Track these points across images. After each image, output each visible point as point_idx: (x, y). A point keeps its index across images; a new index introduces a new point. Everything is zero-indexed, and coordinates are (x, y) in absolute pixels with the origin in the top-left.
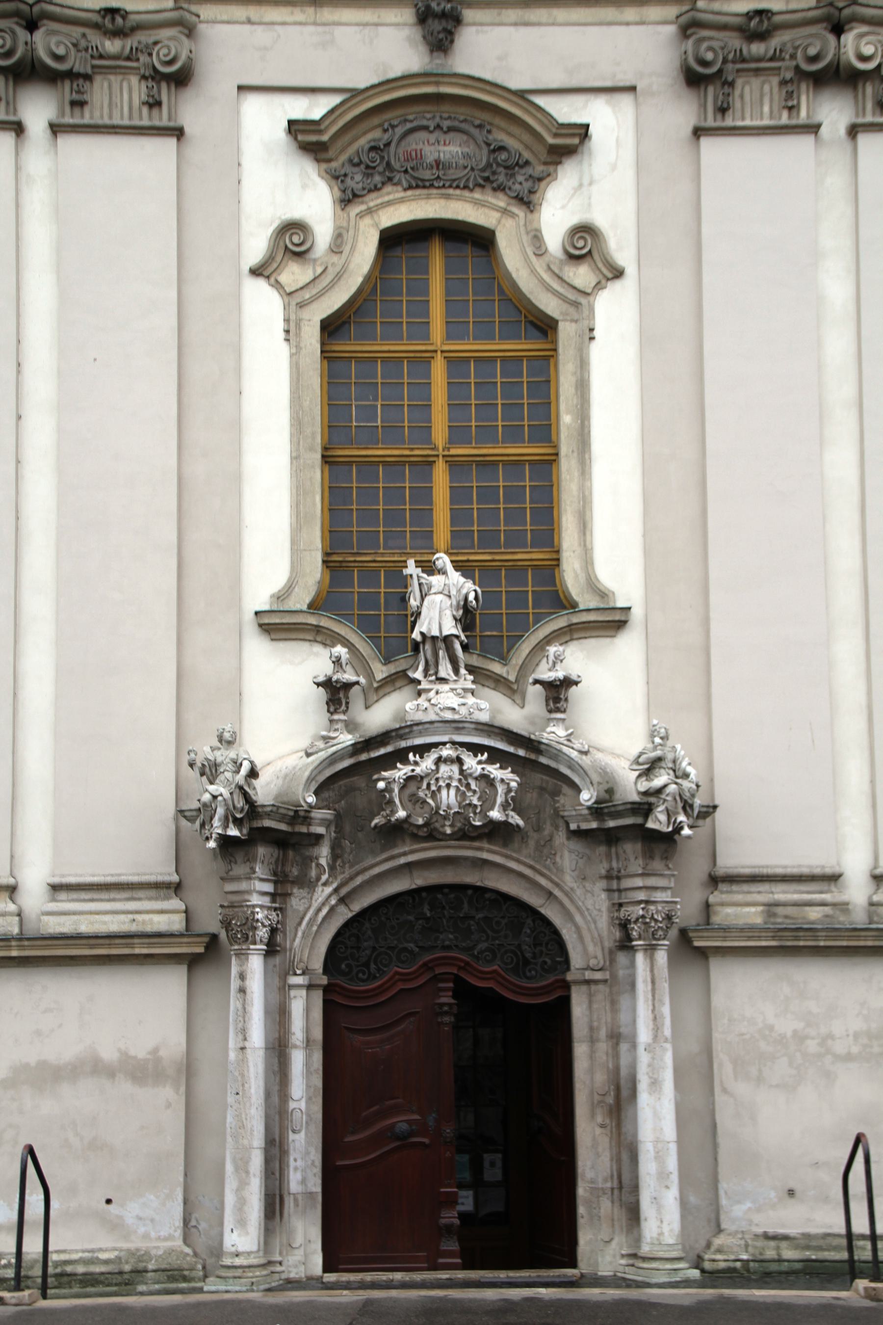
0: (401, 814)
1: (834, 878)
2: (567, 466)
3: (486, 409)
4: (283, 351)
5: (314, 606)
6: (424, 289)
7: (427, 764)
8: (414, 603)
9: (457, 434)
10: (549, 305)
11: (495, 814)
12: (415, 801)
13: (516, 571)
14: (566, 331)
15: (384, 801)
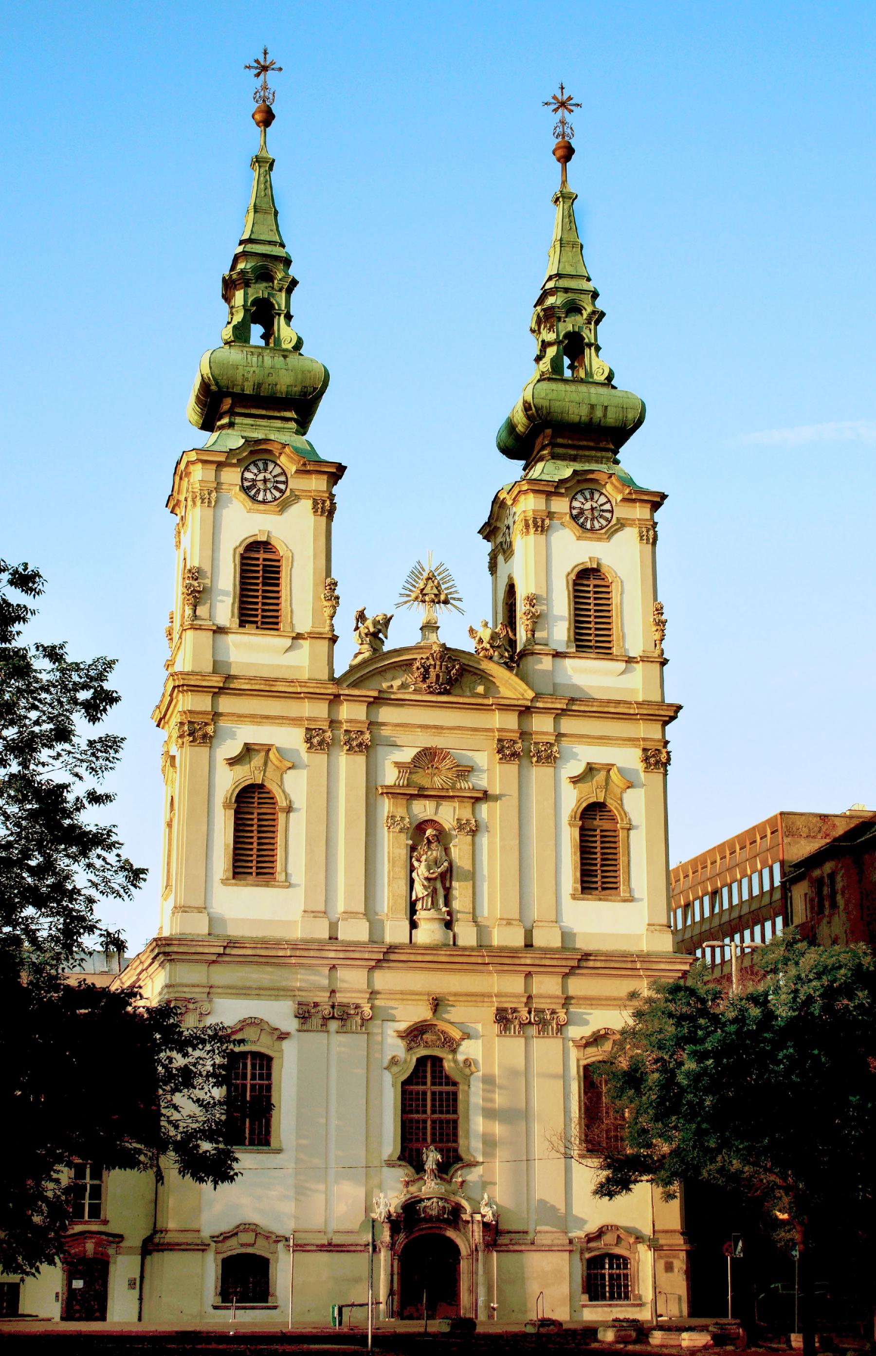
0: (423, 1215)
1: (526, 1232)
2: (461, 1122)
3: (441, 1106)
4: (392, 1089)
5: (399, 1159)
6: (425, 1071)
7: (428, 1203)
8: (425, 1159)
9: (433, 1112)
10: (458, 1079)
11: (446, 1216)
12: (424, 1212)
13: (448, 1150)
14: (462, 1087)
15: (418, 1212)
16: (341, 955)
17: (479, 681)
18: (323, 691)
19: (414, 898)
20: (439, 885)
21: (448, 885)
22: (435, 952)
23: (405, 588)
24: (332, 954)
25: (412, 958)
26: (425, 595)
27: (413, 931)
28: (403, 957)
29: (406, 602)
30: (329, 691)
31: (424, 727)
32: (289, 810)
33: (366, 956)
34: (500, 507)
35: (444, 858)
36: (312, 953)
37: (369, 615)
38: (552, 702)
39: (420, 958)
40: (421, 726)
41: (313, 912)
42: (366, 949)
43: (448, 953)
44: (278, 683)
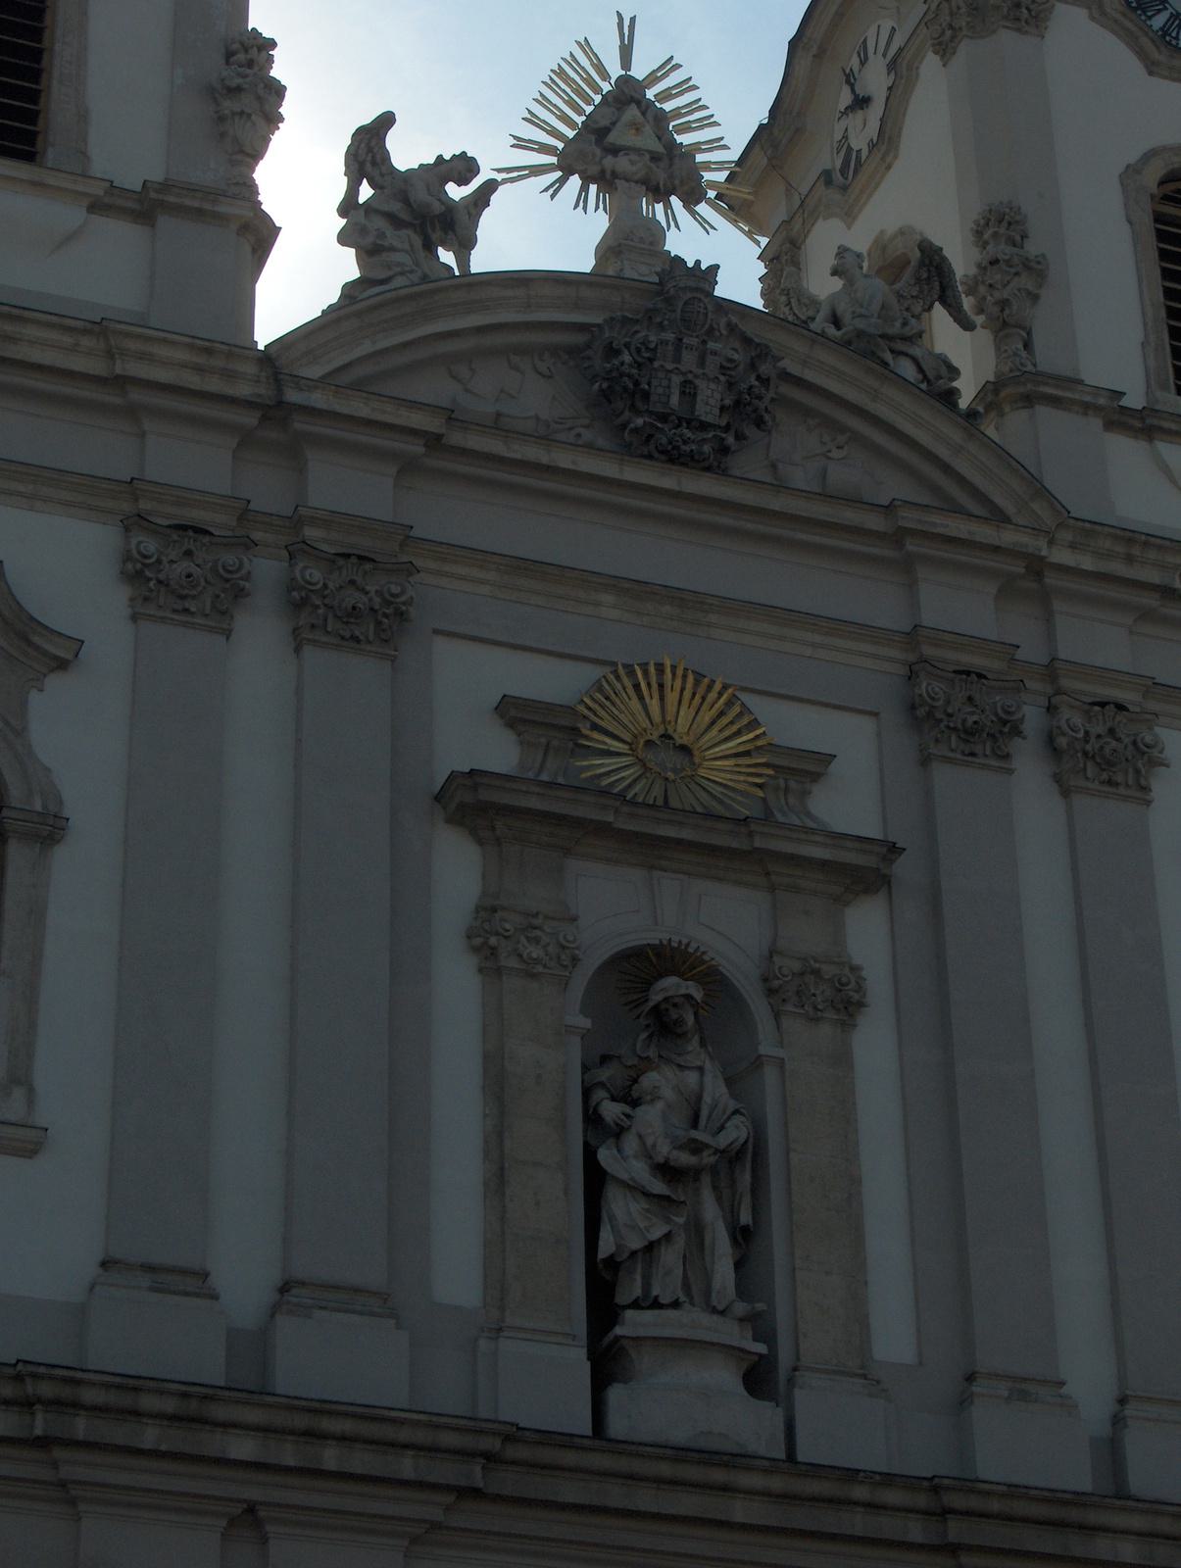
16: (288, 1454)
17: (836, 454)
18: (214, 385)
19: (606, 1246)
20: (711, 1211)
21: (745, 1218)
22: (718, 1476)
23: (532, 120)
24: (243, 1448)
25: (616, 1495)
26: (615, 151)
27: (615, 1394)
28: (570, 1491)
29: (536, 170)
30: (243, 390)
31: (636, 591)
32: (50, 830)
33: (406, 1466)
34: (819, 56)
35: (732, 1105)
36: (150, 1436)
37: (406, 152)
38: (1130, 559)
39: (645, 1499)
40: (619, 585)
41: (149, 1268)
42: (404, 1435)
43: (776, 1483)
44: (30, 331)
